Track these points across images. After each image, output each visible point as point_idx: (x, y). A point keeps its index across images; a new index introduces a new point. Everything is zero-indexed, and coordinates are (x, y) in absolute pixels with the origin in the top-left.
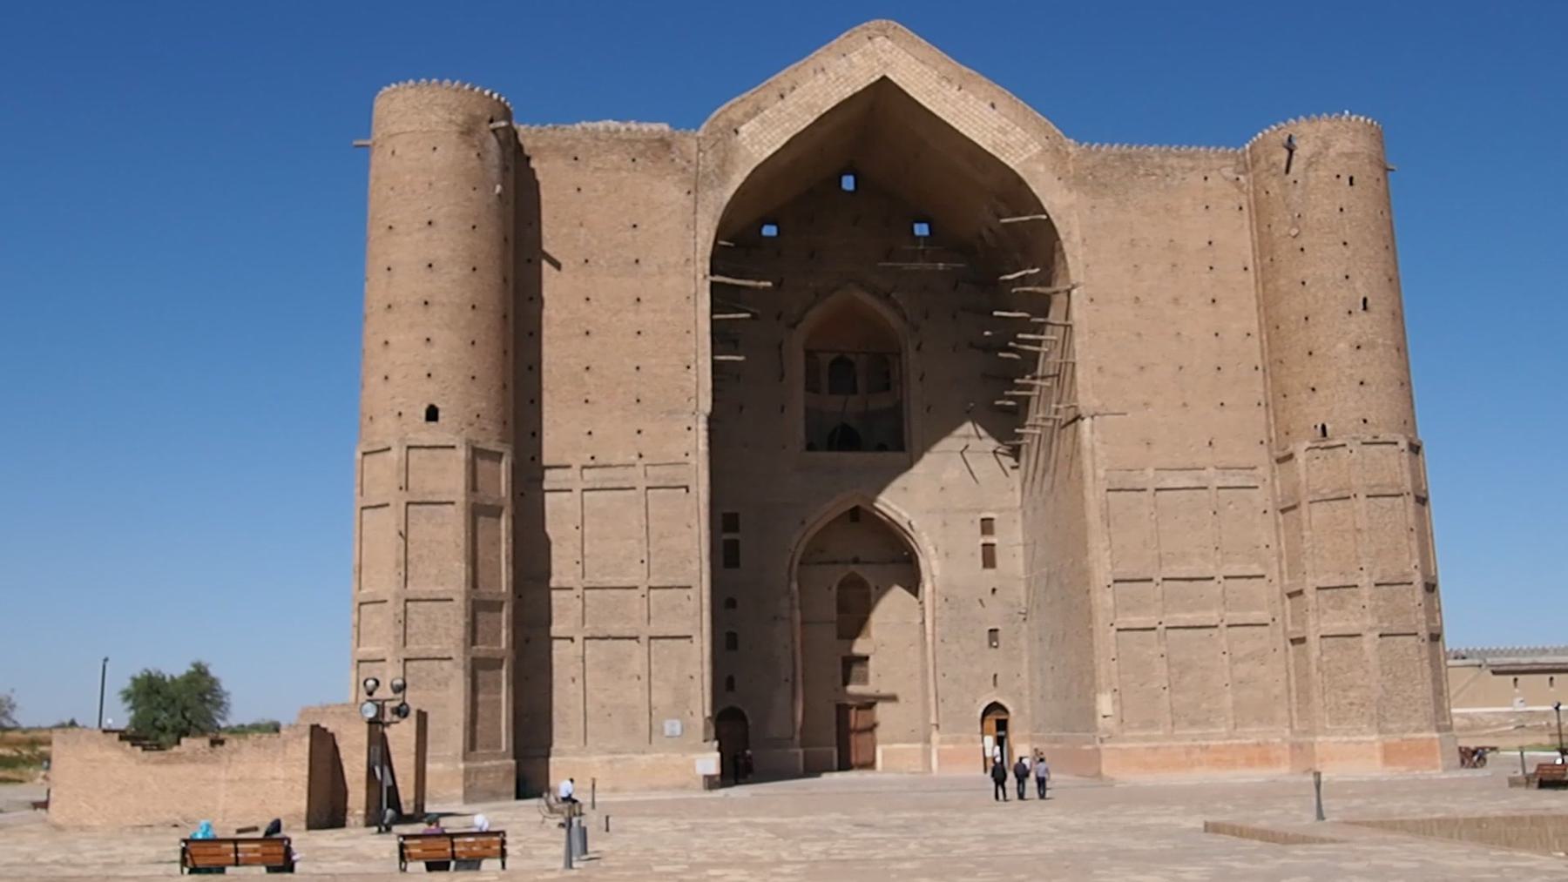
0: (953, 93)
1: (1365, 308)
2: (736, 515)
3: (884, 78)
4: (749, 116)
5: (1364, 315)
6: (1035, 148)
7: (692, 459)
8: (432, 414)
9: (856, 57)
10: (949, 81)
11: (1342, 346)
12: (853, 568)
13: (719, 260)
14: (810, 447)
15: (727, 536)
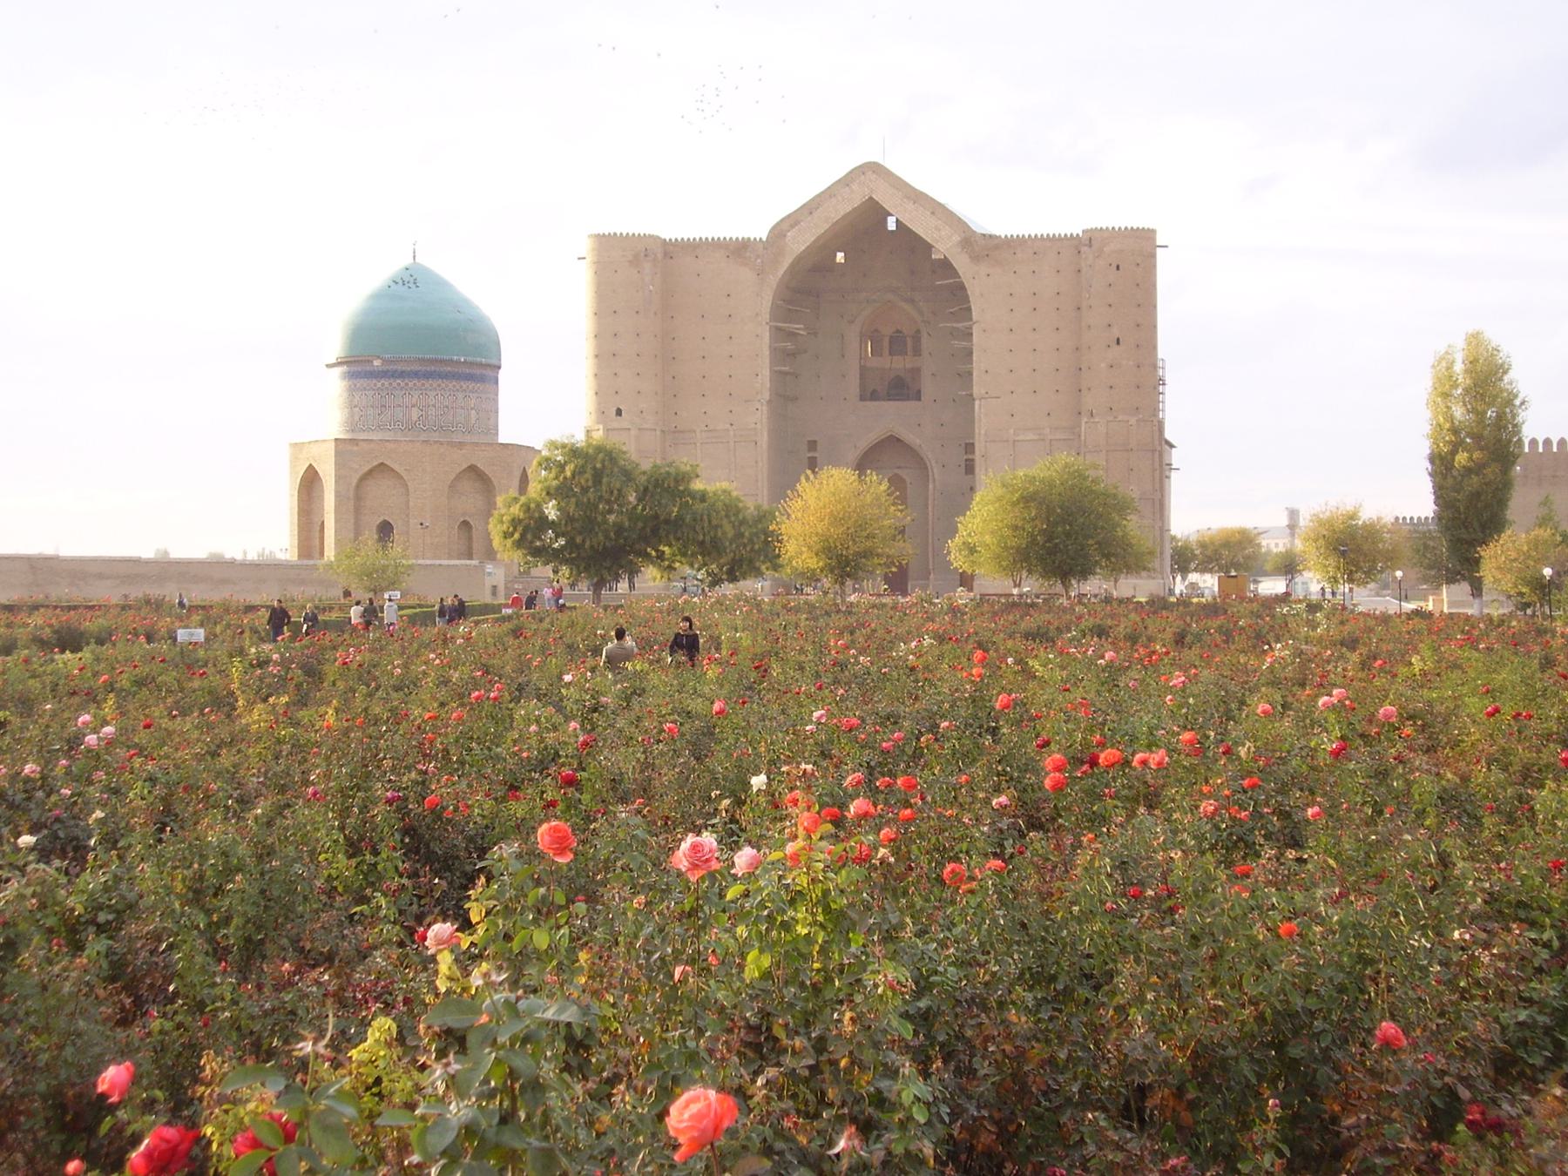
0: (910, 206)
1: (1118, 342)
2: (815, 442)
3: (871, 198)
4: (792, 226)
5: (1116, 348)
6: (956, 238)
7: (759, 426)
8: (619, 412)
9: (855, 186)
10: (908, 198)
11: (1103, 365)
12: (896, 471)
13: (775, 315)
14: (862, 398)
15: (810, 455)
